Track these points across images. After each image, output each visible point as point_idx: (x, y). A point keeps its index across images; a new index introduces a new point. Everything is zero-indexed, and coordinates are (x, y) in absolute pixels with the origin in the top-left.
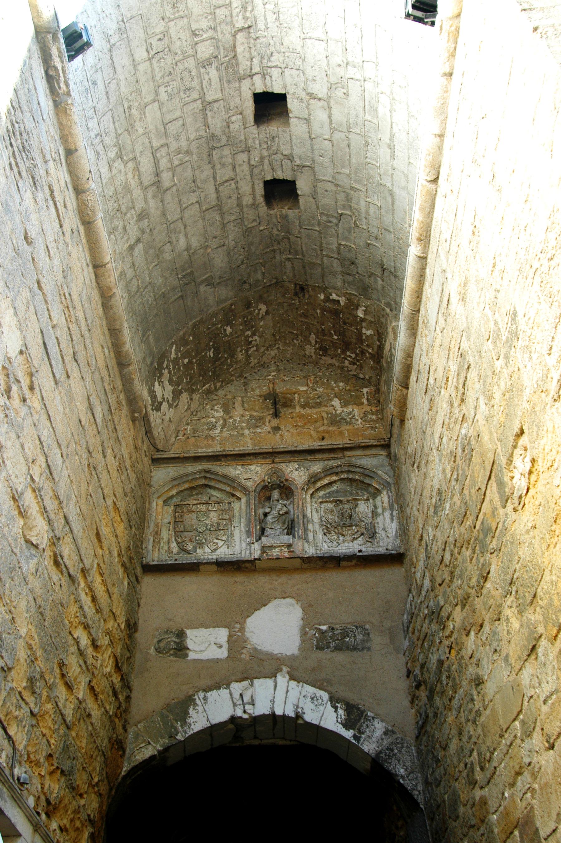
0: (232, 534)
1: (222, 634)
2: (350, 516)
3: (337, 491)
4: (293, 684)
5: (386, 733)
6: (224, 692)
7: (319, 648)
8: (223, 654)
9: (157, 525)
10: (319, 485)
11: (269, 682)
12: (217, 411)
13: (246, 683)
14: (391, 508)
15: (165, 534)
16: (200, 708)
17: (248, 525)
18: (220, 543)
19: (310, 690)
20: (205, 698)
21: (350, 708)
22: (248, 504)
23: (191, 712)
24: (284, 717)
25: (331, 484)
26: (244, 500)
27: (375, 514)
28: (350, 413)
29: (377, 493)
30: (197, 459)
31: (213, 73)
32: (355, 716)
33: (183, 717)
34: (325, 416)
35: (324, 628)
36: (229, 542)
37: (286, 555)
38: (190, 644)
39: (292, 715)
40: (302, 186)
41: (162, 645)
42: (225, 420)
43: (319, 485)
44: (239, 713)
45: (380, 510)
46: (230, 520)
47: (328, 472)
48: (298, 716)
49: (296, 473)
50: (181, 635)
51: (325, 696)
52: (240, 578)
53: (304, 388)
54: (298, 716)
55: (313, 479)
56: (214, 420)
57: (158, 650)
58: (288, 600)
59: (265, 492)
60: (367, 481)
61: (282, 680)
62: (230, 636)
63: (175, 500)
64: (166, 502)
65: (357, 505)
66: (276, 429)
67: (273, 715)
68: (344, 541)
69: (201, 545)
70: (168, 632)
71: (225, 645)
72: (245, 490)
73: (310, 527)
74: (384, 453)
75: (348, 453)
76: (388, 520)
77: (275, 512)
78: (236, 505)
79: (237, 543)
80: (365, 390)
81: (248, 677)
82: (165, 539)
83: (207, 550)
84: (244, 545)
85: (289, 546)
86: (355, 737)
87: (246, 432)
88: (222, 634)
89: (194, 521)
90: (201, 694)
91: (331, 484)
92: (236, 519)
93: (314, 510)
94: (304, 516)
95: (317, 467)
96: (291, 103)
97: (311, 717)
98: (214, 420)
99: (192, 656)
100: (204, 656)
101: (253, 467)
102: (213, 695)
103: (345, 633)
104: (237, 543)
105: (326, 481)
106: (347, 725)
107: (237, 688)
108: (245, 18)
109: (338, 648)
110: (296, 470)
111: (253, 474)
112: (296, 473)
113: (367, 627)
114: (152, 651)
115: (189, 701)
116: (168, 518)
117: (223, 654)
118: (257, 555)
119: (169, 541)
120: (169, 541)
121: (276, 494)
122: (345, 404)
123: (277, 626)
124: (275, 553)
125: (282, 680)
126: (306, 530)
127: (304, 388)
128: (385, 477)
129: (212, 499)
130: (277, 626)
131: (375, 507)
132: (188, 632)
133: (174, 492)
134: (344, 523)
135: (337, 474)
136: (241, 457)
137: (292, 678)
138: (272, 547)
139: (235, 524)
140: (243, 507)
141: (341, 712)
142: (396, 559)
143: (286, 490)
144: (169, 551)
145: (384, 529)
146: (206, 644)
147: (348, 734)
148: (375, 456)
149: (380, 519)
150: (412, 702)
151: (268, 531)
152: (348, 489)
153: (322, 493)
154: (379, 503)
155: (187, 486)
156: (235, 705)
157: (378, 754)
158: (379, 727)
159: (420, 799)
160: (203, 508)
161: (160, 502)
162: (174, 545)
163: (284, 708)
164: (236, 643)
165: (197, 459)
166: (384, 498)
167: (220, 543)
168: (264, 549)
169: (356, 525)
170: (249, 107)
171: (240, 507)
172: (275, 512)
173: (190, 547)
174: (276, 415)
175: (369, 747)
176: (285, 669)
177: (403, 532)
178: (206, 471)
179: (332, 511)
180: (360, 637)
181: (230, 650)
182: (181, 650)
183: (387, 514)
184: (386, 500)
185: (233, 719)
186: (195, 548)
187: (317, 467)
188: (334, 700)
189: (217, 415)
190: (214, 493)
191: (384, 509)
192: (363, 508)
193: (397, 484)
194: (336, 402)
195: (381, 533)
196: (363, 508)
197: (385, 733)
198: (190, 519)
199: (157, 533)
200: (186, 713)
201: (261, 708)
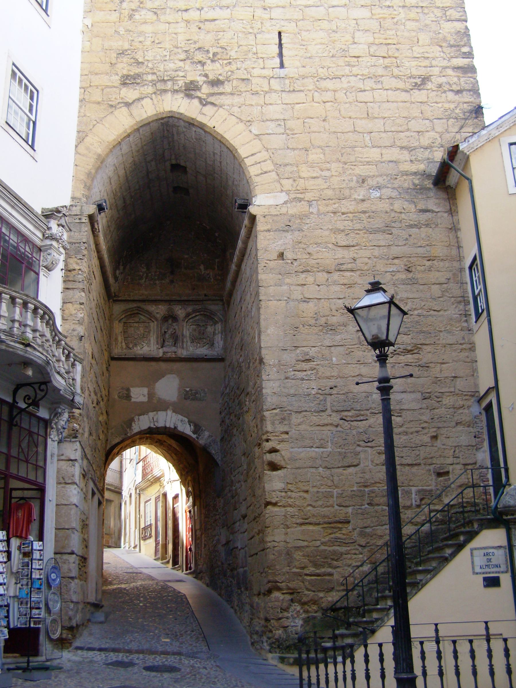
0: (150, 340)
1: (145, 391)
2: (203, 334)
3: (198, 320)
4: (174, 414)
5: (209, 436)
6: (146, 416)
7: (185, 399)
8: (145, 399)
9: (116, 334)
10: (190, 317)
11: (164, 413)
12: (143, 268)
13: (155, 413)
14: (222, 333)
15: (120, 339)
16: (136, 423)
17: (157, 338)
18: (145, 344)
19: (180, 417)
20: (139, 419)
21: (196, 425)
22: (157, 325)
23: (133, 425)
24: (170, 428)
25: (196, 316)
26: (156, 322)
27: (214, 334)
28: (208, 274)
29: (216, 323)
30: (134, 301)
31: (153, 163)
32: (197, 430)
33: (130, 426)
34: (196, 275)
35: (188, 389)
36: (149, 345)
37: (174, 356)
38: (132, 395)
39: (172, 427)
40: (191, 191)
41: (121, 394)
42: (147, 274)
43: (190, 317)
44: (152, 426)
45: (217, 332)
46: (149, 332)
47: (194, 311)
48: (175, 428)
49: (180, 311)
50: (128, 390)
51: (186, 420)
52: (154, 364)
53: (186, 256)
54: (175, 428)
55: (188, 315)
56: (141, 273)
57: (119, 397)
58: (174, 375)
59: (165, 319)
60: (212, 316)
61: (169, 412)
62: (149, 391)
63: (124, 320)
64: (120, 321)
65: (206, 328)
66: (172, 282)
67: (166, 427)
68: (199, 347)
69: (136, 345)
70: (122, 388)
71: (147, 396)
72: (156, 319)
73: (185, 340)
74: (221, 303)
75: (205, 302)
76: (220, 339)
77: (169, 332)
78: (152, 324)
79: (152, 345)
80: (217, 260)
81: (156, 409)
82: (120, 341)
83: (139, 348)
84: (155, 348)
85: (175, 352)
86: (197, 438)
87: (157, 282)
88: (145, 391)
89: (133, 332)
90: (137, 417)
91: (196, 316)
92: (152, 333)
93: (187, 330)
94: (183, 335)
95: (190, 309)
96: (188, 169)
97: (180, 428)
98: (141, 273)
99: (133, 400)
100: (138, 400)
101: (160, 306)
102: (142, 417)
103: (196, 393)
104: (152, 345)
105: (194, 315)
106: (194, 432)
107: (151, 414)
108: (169, 146)
109: (193, 399)
110: (181, 309)
111: (160, 310)
112: (180, 311)
113: (206, 390)
114: (116, 397)
115: (132, 420)
116: (121, 329)
117: (145, 399)
118: (161, 355)
119: (121, 343)
120: (121, 343)
121: (170, 321)
122: (206, 269)
123: (168, 387)
124: (169, 355)
125: (169, 412)
126: (183, 342)
127: (186, 256)
128: (221, 317)
129: (141, 320)
130: (168, 387)
131: (215, 330)
132: (131, 389)
133: (123, 316)
134: (200, 337)
135: (199, 312)
136: (155, 302)
137: (174, 411)
138: (167, 352)
139: (152, 334)
140: (155, 327)
141: (192, 427)
142: (221, 360)
143: (175, 319)
144: (122, 348)
145: (218, 342)
146: (139, 394)
147: (194, 436)
148: (217, 304)
149: (216, 337)
150: (221, 424)
151: (166, 343)
152: (204, 319)
153: (191, 320)
154: (217, 328)
155: (129, 313)
156: (150, 422)
157: (205, 444)
158: (207, 434)
159: (219, 463)
160: (136, 325)
161: (117, 322)
162: (124, 344)
163: (170, 424)
164: (151, 395)
165: (134, 301)
166: (219, 327)
167: (145, 344)
168: (164, 353)
169: (205, 339)
170: (169, 167)
171: (153, 325)
172: (169, 332)
173: (131, 346)
174: (172, 273)
175: (202, 442)
176: (171, 407)
177: (225, 348)
178: (138, 307)
179: (195, 330)
180: (202, 394)
181: (148, 398)
182: (128, 397)
183: (220, 335)
184: (220, 327)
185: (150, 428)
186: (133, 347)
187: (190, 309)
188: (190, 422)
189: (143, 270)
190: (142, 317)
191: (219, 332)
192: (210, 329)
193: (225, 321)
194: (202, 267)
195: (216, 345)
196: (210, 329)
197: (209, 436)
198: (131, 331)
199: (116, 339)
200: (131, 425)
201: (161, 424)
